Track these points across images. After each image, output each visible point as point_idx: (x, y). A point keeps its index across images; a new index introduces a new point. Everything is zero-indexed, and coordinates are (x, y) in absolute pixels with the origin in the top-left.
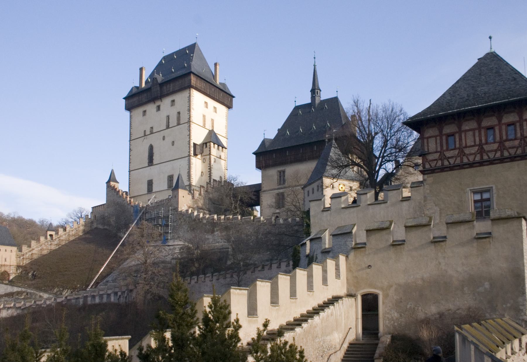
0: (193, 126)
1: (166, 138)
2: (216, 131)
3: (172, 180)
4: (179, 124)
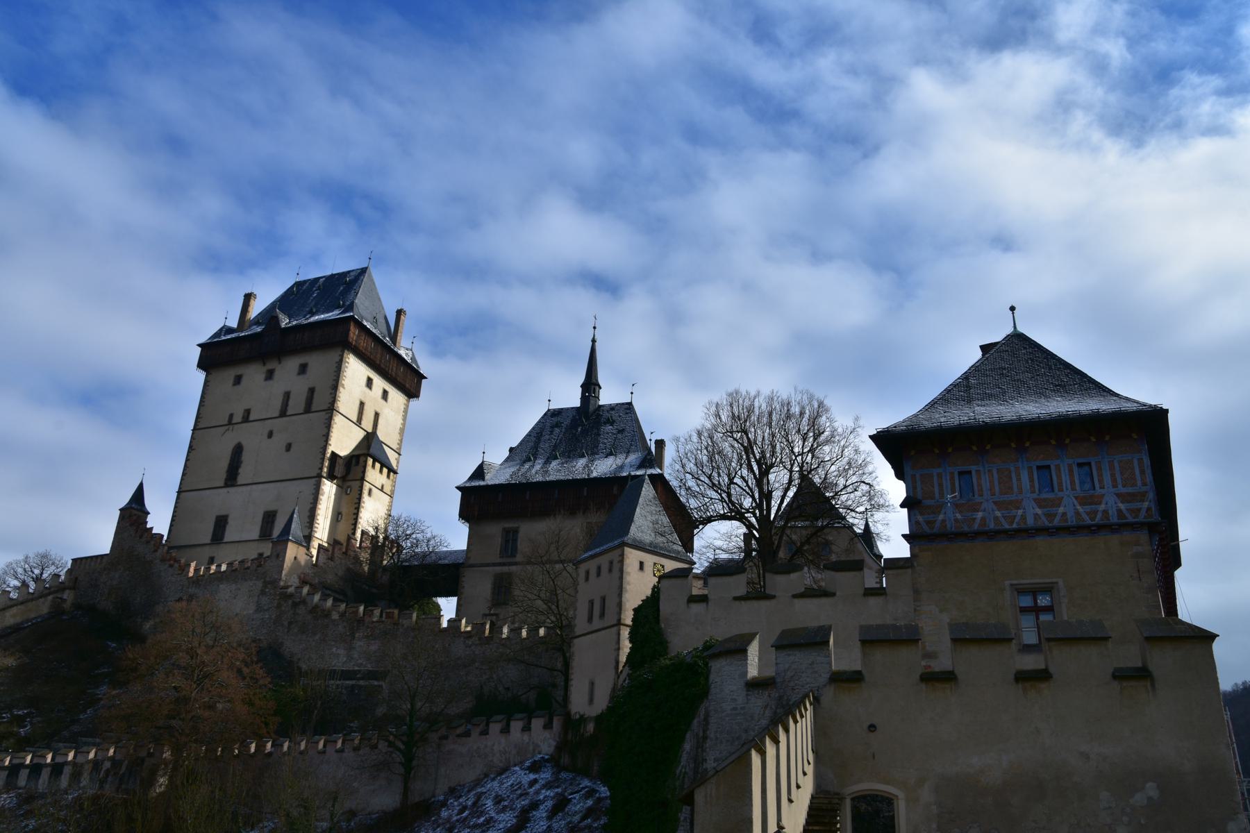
0: (338, 421)
1: (275, 434)
2: (381, 434)
3: (273, 522)
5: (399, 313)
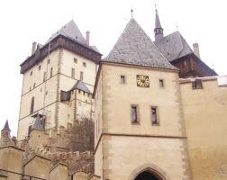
4: (51, 77)
5: (88, 33)
